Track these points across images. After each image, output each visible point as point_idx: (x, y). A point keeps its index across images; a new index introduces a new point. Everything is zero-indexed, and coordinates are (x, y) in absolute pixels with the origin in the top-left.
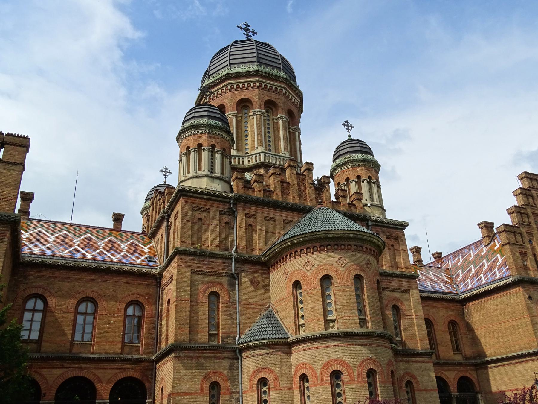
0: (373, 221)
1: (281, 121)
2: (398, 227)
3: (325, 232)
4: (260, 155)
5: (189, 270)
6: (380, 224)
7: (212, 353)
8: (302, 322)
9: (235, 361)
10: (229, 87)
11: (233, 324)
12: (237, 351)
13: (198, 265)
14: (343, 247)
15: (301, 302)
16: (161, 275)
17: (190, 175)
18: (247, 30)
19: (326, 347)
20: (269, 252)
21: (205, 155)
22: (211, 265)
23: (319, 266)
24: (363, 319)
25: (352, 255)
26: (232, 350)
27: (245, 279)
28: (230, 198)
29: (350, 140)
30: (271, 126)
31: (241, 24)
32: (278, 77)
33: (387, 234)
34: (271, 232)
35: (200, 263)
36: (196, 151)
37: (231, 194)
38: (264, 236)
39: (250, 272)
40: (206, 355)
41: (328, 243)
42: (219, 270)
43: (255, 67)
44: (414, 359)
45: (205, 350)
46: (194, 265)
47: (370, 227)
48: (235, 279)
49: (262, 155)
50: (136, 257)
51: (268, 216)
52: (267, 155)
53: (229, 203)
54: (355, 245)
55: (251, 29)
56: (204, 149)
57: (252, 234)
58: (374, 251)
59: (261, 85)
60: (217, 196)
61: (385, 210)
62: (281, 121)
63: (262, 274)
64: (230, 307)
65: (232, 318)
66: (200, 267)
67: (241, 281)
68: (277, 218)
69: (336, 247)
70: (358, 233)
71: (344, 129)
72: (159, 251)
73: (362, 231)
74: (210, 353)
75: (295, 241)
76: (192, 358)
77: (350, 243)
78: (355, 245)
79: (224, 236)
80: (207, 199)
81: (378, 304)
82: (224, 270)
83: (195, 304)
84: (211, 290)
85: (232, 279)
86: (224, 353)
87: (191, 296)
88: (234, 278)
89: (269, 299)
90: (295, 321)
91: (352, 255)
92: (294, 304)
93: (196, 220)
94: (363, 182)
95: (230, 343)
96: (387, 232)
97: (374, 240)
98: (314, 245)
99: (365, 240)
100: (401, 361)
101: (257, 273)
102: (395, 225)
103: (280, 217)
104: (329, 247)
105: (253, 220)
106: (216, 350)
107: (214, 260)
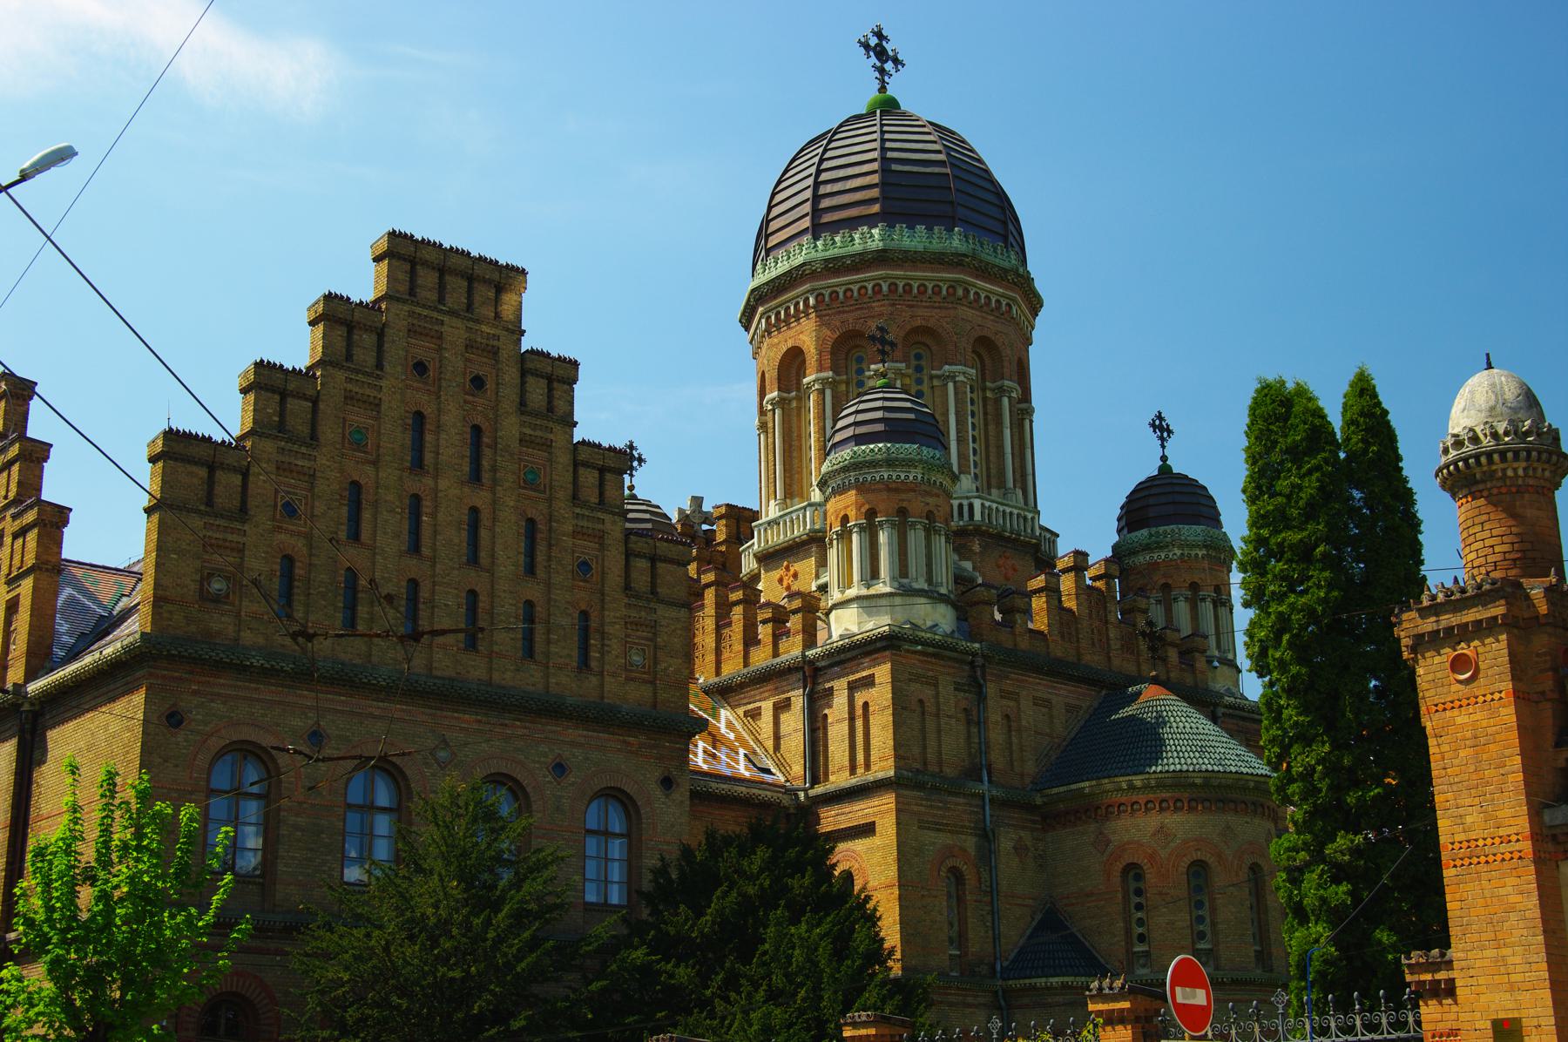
1: (1006, 401)
4: (971, 506)
8: (1139, 948)
10: (885, 288)
14: (1232, 806)
15: (1139, 907)
16: (808, 811)
17: (882, 588)
18: (881, 54)
20: (1062, 789)
21: (916, 538)
27: (1006, 843)
28: (974, 654)
29: (1165, 469)
30: (979, 408)
31: (866, 31)
32: (1006, 271)
36: (893, 525)
37: (977, 645)
43: (956, 242)
49: (977, 503)
50: (728, 756)
51: (1039, 694)
52: (987, 504)
53: (972, 663)
54: (1254, 803)
55: (888, 47)
56: (913, 525)
59: (967, 291)
60: (954, 649)
62: (1006, 401)
71: (1152, 438)
72: (770, 744)
75: (1138, 783)
78: (1254, 803)
80: (934, 655)
84: (950, 863)
88: (986, 837)
94: (1203, 600)
104: (1207, 804)
105: (1012, 704)
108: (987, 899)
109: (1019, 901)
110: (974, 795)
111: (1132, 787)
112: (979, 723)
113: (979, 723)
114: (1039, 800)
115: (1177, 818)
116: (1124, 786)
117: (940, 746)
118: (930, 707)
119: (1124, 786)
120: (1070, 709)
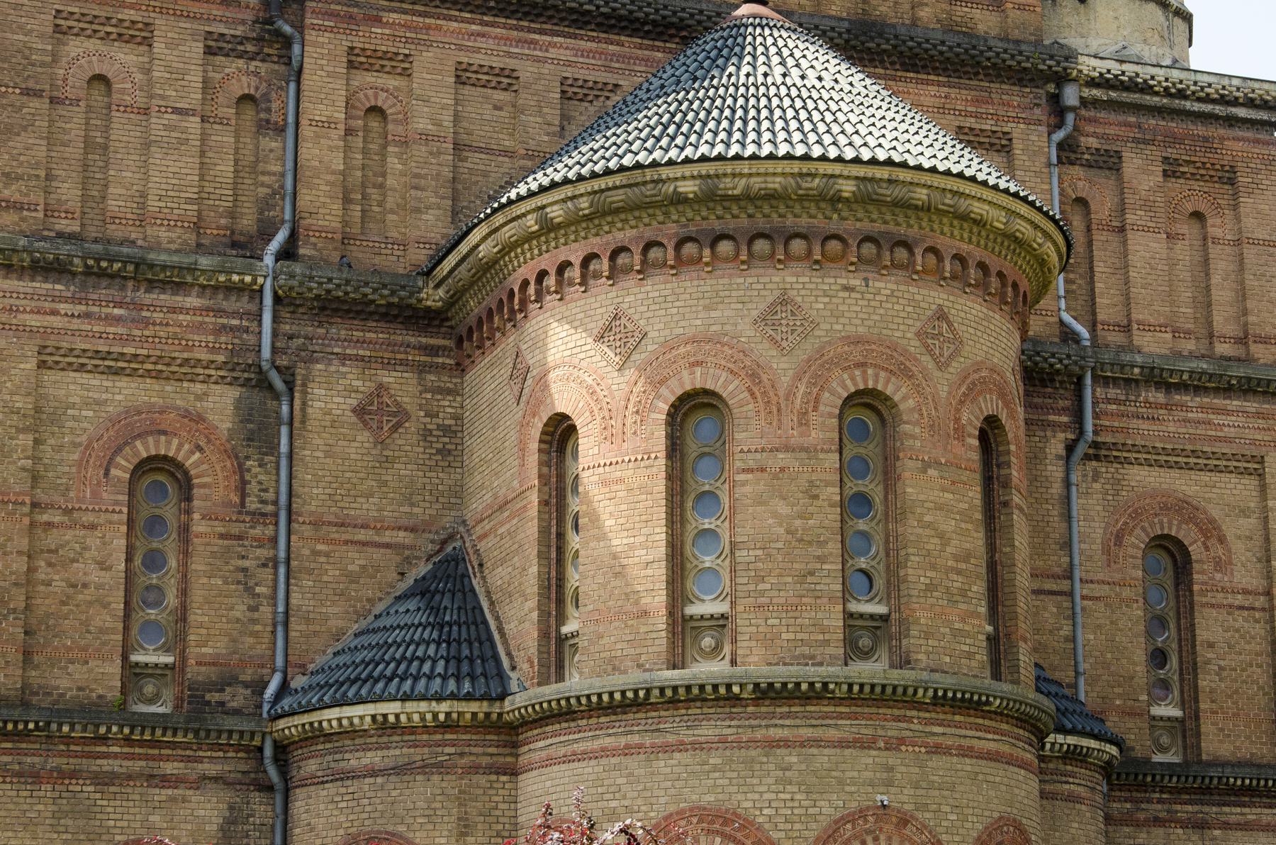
0: (1092, 83)
2: (1242, 112)
3: (704, 168)
5: (31, 350)
6: (1135, 97)
7: (141, 757)
9: (256, 797)
11: (254, 621)
12: (268, 751)
13: (76, 324)
19: (667, 749)
22: (147, 323)
23: (668, 346)
24: (872, 617)
25: (846, 288)
26: (238, 748)
27: (331, 394)
33: (1171, 152)
34: (488, 150)
35: (88, 315)
38: (447, 172)
39: (362, 359)
40: (106, 765)
41: (718, 226)
42: (188, 348)
44: (1233, 813)
45: (104, 739)
46: (56, 321)
47: (1070, 117)
48: (277, 396)
51: (478, 59)
54: (868, 239)
57: (384, 160)
58: (982, 266)
61: (1187, 18)
63: (422, 369)
64: (240, 538)
65: (249, 590)
66: (86, 335)
67: (304, 404)
68: (526, 71)
69: (761, 246)
70: (883, 173)
73: (904, 165)
74: (131, 757)
75: (556, 213)
76: (35, 777)
77: (834, 225)
78: (868, 239)
79: (224, 169)
81: (977, 540)
82: (213, 350)
83: (57, 519)
84: (143, 449)
85: (257, 396)
86: (199, 760)
87: (35, 478)
89: (458, 495)
90: (544, 615)
91: (846, 288)
92: (544, 531)
93: (75, 84)
95: (237, 712)
96: (1175, 140)
97: (978, 209)
98: (649, 234)
99: (927, 208)
100: (1157, 821)
101: (389, 365)
102: (1223, 100)
103: (547, 69)
105: (392, 82)
106: (154, 743)
107: (165, 298)
108: (269, 531)
109: (362, 535)
110: (231, 289)
111: (548, 227)
112: (281, 130)
113: (281, 130)
114: (433, 297)
115: (657, 287)
116: (531, 223)
117: (146, 177)
118: (125, 90)
119: (531, 223)
120: (573, 92)
